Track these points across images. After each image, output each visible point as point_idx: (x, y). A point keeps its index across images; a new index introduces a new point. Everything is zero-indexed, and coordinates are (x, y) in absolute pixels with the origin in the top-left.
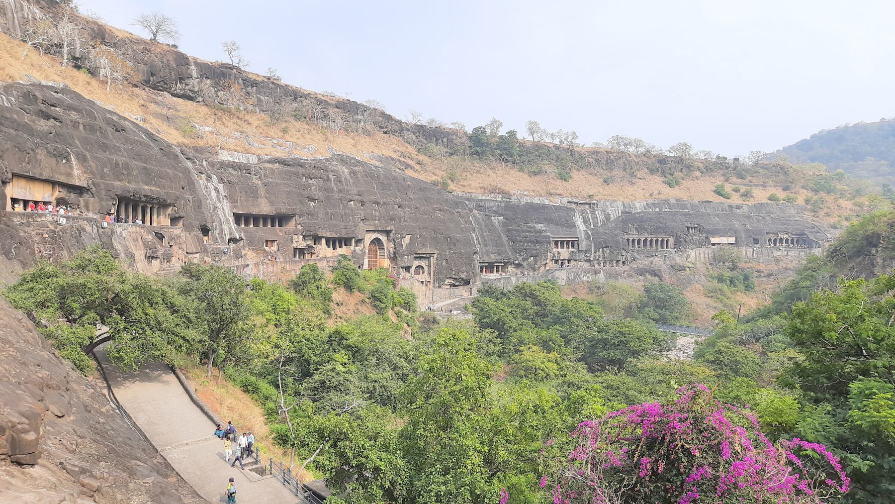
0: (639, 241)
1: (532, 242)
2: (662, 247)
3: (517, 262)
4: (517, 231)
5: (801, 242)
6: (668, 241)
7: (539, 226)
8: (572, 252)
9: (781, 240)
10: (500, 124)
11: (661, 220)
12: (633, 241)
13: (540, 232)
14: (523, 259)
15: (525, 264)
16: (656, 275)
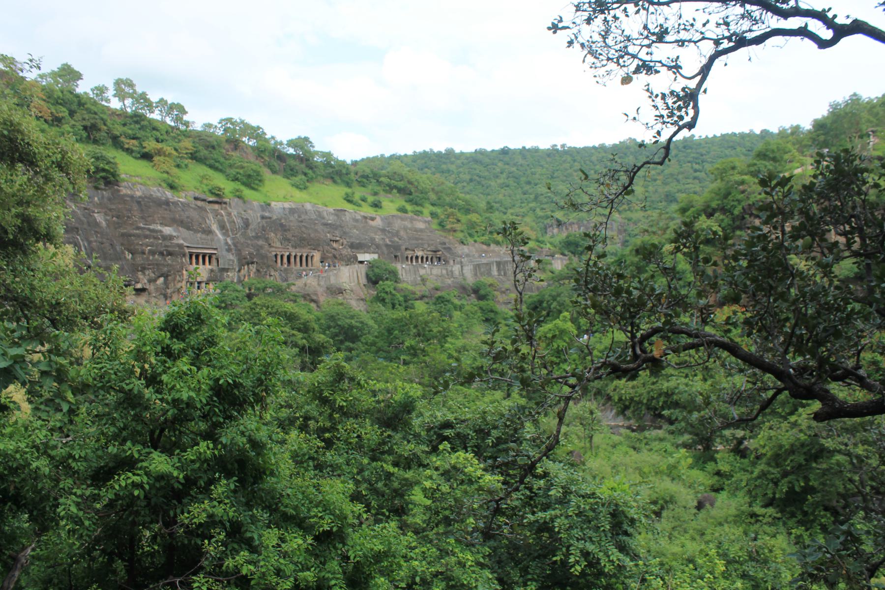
0: (282, 256)
1: (161, 254)
2: (307, 265)
3: (139, 286)
4: (138, 236)
5: (434, 259)
6: (312, 257)
7: (168, 230)
8: (212, 271)
9: (417, 257)
10: (78, 76)
11: (303, 229)
12: (276, 256)
13: (171, 238)
14: (150, 281)
15: (151, 287)
16: (313, 301)
